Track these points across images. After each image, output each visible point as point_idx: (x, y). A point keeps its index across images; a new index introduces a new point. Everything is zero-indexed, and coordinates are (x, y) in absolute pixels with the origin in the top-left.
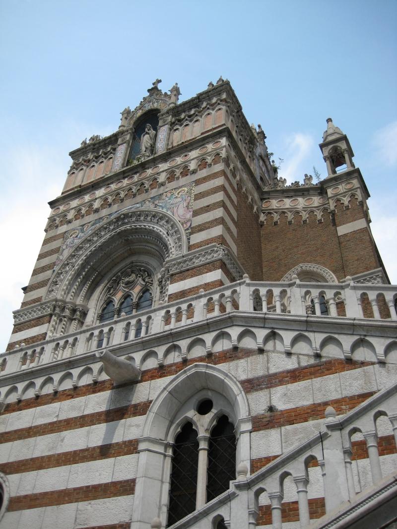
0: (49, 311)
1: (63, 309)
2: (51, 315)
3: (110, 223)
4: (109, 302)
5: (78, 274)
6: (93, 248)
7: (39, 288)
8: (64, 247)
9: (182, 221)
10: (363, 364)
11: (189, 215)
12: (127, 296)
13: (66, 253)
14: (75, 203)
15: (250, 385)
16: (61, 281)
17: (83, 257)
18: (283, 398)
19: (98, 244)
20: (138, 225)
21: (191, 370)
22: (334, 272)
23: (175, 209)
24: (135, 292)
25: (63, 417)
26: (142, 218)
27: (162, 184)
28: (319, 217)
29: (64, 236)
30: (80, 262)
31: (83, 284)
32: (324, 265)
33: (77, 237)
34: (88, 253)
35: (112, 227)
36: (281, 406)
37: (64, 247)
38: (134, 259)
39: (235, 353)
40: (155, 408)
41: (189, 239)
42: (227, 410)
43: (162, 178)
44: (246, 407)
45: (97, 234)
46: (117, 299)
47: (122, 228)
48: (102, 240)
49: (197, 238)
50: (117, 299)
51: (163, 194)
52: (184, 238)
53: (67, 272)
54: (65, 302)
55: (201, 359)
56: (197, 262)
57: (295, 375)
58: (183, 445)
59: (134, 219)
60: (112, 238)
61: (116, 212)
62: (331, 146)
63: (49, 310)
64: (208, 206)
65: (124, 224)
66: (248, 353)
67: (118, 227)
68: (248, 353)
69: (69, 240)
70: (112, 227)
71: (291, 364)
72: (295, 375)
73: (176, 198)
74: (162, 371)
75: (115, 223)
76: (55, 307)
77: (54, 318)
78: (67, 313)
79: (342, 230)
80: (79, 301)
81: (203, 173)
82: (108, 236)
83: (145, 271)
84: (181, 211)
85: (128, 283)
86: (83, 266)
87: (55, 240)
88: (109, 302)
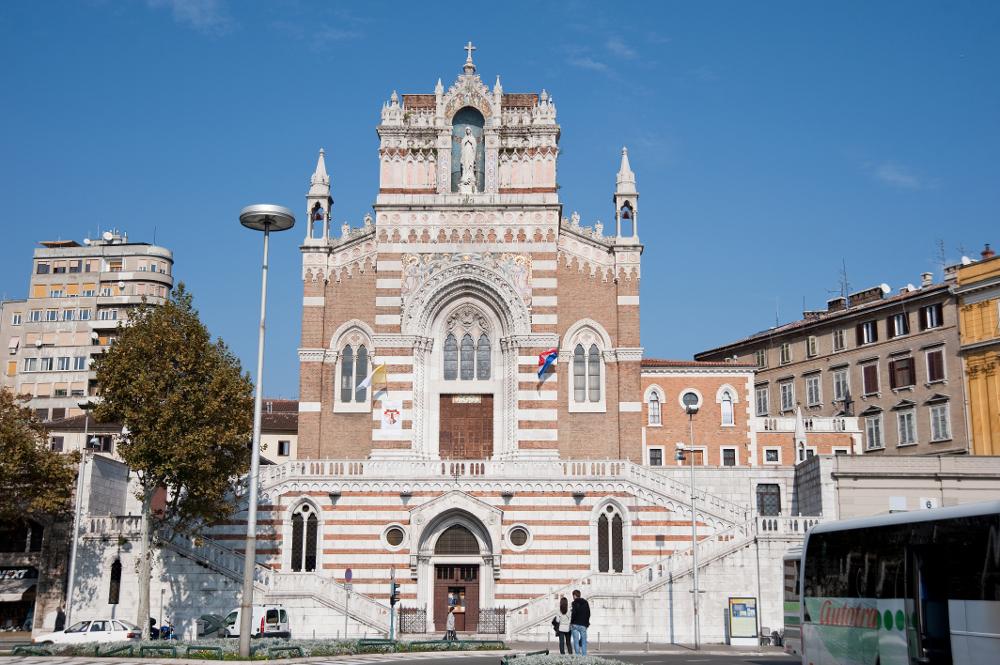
4: (450, 335)
8: (407, 274)
10: (668, 510)
11: (529, 292)
14: (405, 217)
15: (631, 509)
17: (430, 295)
18: (643, 516)
21: (608, 497)
22: (610, 334)
24: (476, 334)
28: (605, 278)
29: (401, 256)
30: (427, 299)
33: (418, 265)
35: (456, 271)
36: (641, 519)
38: (470, 299)
39: (624, 494)
40: (594, 509)
42: (620, 513)
43: (501, 233)
44: (628, 517)
46: (459, 335)
47: (467, 276)
49: (538, 319)
51: (501, 253)
55: (611, 493)
57: (647, 509)
58: (602, 523)
60: (455, 283)
65: (467, 272)
66: (630, 495)
68: (630, 495)
71: (645, 504)
72: (647, 509)
74: (595, 494)
77: (415, 351)
78: (423, 346)
79: (622, 300)
80: (426, 333)
81: (539, 247)
84: (522, 284)
88: (450, 335)
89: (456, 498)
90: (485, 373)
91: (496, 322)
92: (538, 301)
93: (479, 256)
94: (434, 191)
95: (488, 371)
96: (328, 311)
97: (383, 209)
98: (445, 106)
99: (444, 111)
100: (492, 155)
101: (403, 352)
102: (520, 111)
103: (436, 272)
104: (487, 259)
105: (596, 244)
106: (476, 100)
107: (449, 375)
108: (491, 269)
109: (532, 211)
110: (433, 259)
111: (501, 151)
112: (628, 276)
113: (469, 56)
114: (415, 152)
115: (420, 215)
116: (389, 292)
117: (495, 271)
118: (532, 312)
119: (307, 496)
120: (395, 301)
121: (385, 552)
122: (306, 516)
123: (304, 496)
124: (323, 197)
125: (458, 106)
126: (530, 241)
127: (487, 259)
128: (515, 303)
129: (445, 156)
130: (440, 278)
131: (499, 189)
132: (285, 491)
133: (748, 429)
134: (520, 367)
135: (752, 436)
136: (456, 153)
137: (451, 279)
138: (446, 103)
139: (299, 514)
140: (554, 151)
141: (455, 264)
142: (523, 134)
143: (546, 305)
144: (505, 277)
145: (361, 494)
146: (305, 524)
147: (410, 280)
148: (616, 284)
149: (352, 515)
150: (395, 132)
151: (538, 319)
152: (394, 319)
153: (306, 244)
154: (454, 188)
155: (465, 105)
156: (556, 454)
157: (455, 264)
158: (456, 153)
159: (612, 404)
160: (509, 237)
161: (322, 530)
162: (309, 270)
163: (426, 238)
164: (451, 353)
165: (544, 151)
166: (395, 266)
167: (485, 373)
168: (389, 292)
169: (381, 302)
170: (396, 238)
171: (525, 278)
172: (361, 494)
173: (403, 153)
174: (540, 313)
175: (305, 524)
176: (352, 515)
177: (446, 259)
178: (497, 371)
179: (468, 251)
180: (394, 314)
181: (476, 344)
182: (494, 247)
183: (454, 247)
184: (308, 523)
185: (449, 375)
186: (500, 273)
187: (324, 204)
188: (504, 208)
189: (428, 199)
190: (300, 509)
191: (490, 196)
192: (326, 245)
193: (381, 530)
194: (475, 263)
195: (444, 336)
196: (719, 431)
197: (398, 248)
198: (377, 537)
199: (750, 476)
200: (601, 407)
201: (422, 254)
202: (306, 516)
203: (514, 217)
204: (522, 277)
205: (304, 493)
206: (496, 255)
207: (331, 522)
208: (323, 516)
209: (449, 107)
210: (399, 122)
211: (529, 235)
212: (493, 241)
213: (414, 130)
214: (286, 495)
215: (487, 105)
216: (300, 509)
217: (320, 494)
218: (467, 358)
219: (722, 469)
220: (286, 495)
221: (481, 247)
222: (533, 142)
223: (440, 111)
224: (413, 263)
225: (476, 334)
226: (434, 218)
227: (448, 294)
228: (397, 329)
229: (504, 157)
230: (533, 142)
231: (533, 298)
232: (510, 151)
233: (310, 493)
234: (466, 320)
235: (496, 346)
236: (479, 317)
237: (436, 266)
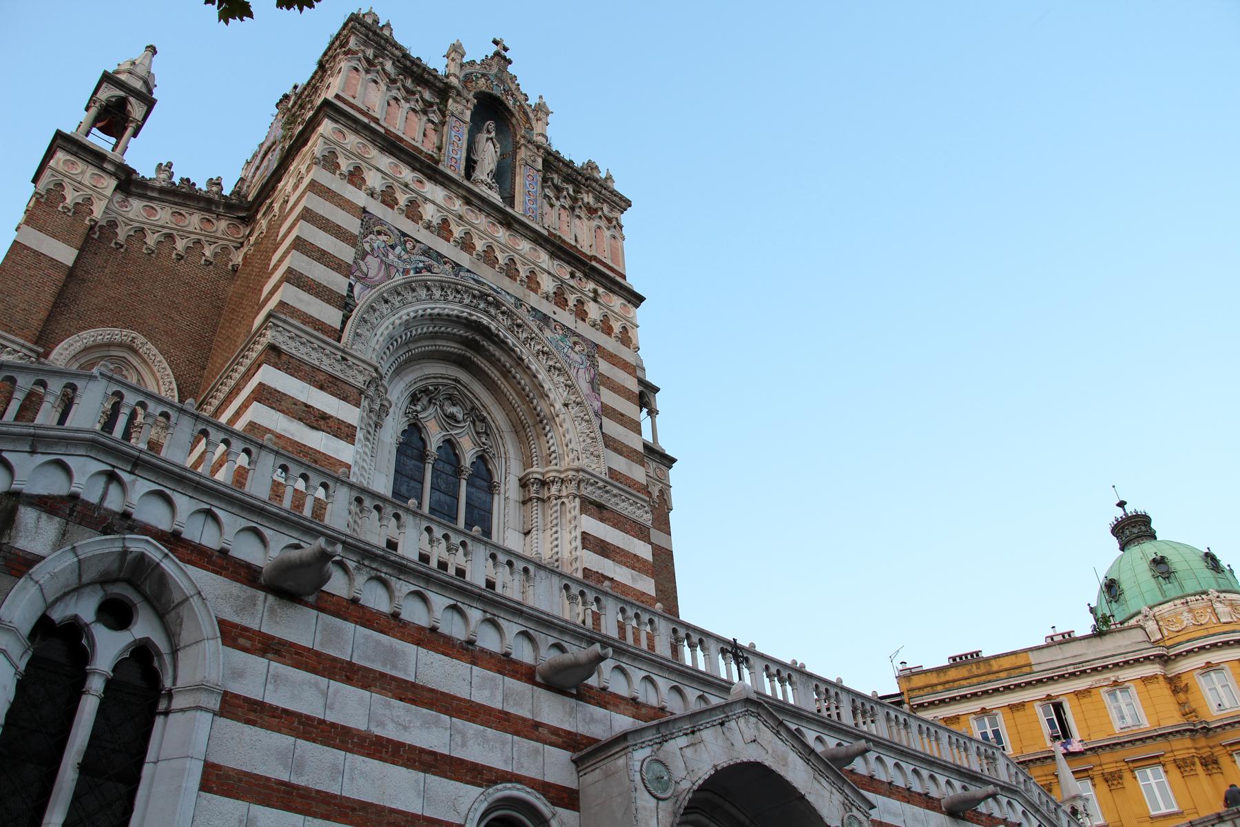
0: (359, 381)
7: (317, 295)
12: (450, 443)
20: (511, 340)
38: (464, 376)
45: (442, 289)
47: (485, 320)
61: (468, 271)
63: (361, 378)
64: (623, 415)
65: (486, 312)
70: (467, 301)
75: (474, 296)
85: (452, 417)
91: (510, 446)
97: (342, 119)
103: (426, 275)
119: (154, 552)
122: (108, 647)
123: (138, 545)
128: (574, 410)
130: (437, 293)
132: (53, 484)
134: (585, 536)
137: (454, 309)
139: (74, 632)
145: (393, 624)
146: (96, 685)
149: (352, 707)
160: (559, 298)
161: (183, 741)
162: (60, 185)
172: (393, 624)
175: (96, 685)
176: (352, 707)
177: (448, 267)
183: (464, 259)
184: (110, 684)
190: (86, 609)
201: (404, 235)
202: (108, 647)
205: (126, 522)
206: (545, 319)
207: (235, 707)
208: (204, 663)
214: (46, 504)
216: (86, 609)
217: (220, 562)
220: (46, 504)
225: (468, 451)
227: (434, 336)
233: (173, 540)
235: (510, 489)
236: (477, 417)
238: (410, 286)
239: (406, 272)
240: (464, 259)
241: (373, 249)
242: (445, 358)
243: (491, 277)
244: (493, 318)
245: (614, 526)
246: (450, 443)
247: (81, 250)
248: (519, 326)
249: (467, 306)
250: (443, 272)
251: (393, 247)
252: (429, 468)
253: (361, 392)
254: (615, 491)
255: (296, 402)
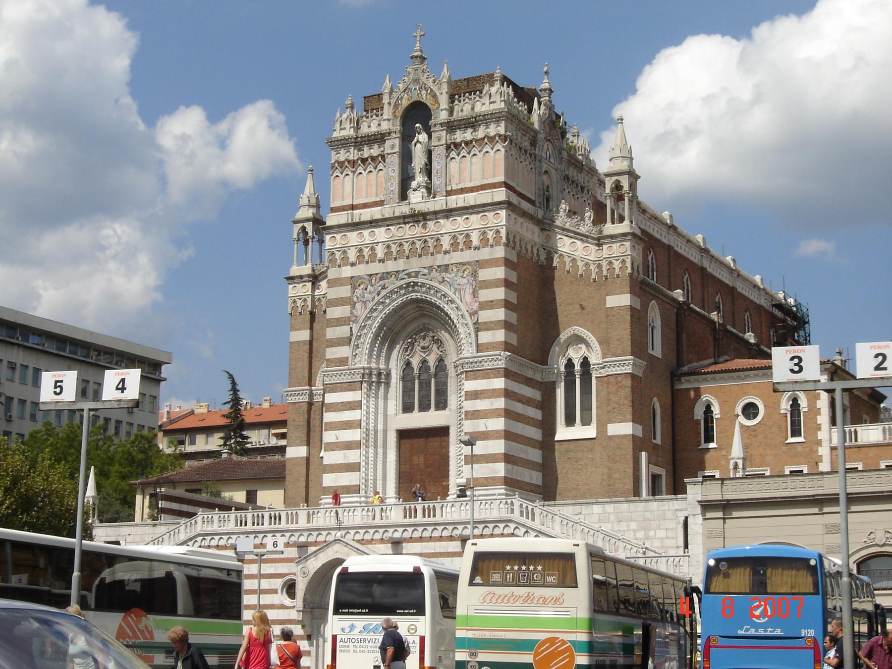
1: (370, 374)
2: (361, 382)
3: (401, 287)
4: (408, 364)
5: (376, 335)
6: (387, 311)
7: (339, 345)
9: (471, 311)
11: (475, 306)
12: (424, 362)
13: (361, 311)
16: (363, 343)
17: (379, 320)
19: (391, 307)
22: (600, 343)
23: (462, 292)
24: (432, 360)
25: (438, 551)
26: (432, 292)
27: (446, 252)
28: (593, 276)
31: (382, 344)
32: (592, 332)
34: (382, 315)
35: (402, 292)
37: (355, 299)
38: (426, 320)
41: (477, 336)
43: (446, 242)
46: (415, 362)
47: (414, 295)
48: (395, 304)
50: (415, 362)
52: (473, 336)
53: (366, 334)
54: (370, 369)
56: (486, 366)
59: (424, 289)
62: (614, 178)
65: (414, 291)
67: (409, 293)
69: (359, 291)
73: (462, 277)
76: (363, 375)
77: (365, 385)
81: (485, 254)
82: (400, 301)
83: (438, 340)
84: (468, 297)
85: (423, 348)
86: (380, 328)
87: (341, 285)
89: (337, 547)
90: (442, 404)
92: (486, 316)
93: (426, 271)
94: (381, 203)
95: (446, 401)
96: (315, 344)
98: (392, 105)
99: (391, 111)
100: (439, 153)
101: (350, 386)
102: (472, 96)
104: (434, 274)
105: (583, 237)
106: (424, 92)
107: (407, 408)
108: (436, 284)
109: (478, 213)
110: (382, 279)
111: (448, 148)
112: (617, 271)
113: (418, 45)
114: (364, 161)
115: (366, 233)
116: (339, 322)
117: (441, 287)
118: (477, 330)
120: (342, 331)
121: (283, 607)
124: (307, 220)
125: (405, 103)
126: (476, 248)
127: (434, 274)
129: (394, 162)
131: (447, 192)
133: (819, 443)
135: (824, 451)
136: (406, 157)
138: (393, 101)
140: (504, 138)
141: (403, 282)
142: (472, 123)
143: (493, 319)
144: (450, 293)
147: (358, 306)
148: (604, 283)
150: (343, 143)
151: (485, 337)
152: (343, 351)
153: (291, 275)
154: (403, 196)
155: (414, 100)
156: (503, 491)
157: (403, 282)
158: (406, 157)
159: (602, 428)
160: (455, 245)
163: (373, 257)
164: (409, 384)
165: (491, 139)
166: (344, 291)
167: (442, 404)
168: (339, 322)
169: (332, 333)
170: (345, 261)
171: (471, 290)
173: (353, 163)
174: (487, 329)
178: (453, 400)
179: (415, 265)
180: (344, 345)
181: (433, 370)
182: (441, 259)
183: (400, 264)
185: (407, 408)
186: (444, 288)
187: (309, 227)
188: (448, 213)
189: (375, 213)
191: (439, 203)
192: (310, 272)
193: (278, 583)
194: (420, 280)
195: (401, 364)
196: (784, 448)
197: (347, 272)
198: (275, 591)
199: (676, 507)
200: (590, 432)
201: (370, 275)
203: (460, 223)
204: (469, 290)
206: (446, 268)
209: (396, 106)
210: (349, 132)
211: (475, 239)
212: (439, 252)
213: (362, 137)
215: (435, 96)
218: (425, 387)
219: (646, 501)
221: (427, 261)
222: (481, 133)
223: (387, 112)
224: (362, 286)
226: (381, 234)
228: (343, 361)
229: (453, 154)
230: (481, 133)
231: (480, 312)
232: (457, 145)
234: (422, 344)
237: (384, 288)
238: (372, 310)
239: (373, 299)
240: (400, 264)
241: (358, 298)
242: (416, 318)
243: (415, 265)
244: (418, 292)
245: (482, 378)
246: (424, 362)
247: (311, 328)
248: (429, 288)
249: (404, 295)
250: (392, 284)
251: (366, 289)
252: (417, 381)
253: (361, 382)
254: (480, 359)
255: (338, 404)
